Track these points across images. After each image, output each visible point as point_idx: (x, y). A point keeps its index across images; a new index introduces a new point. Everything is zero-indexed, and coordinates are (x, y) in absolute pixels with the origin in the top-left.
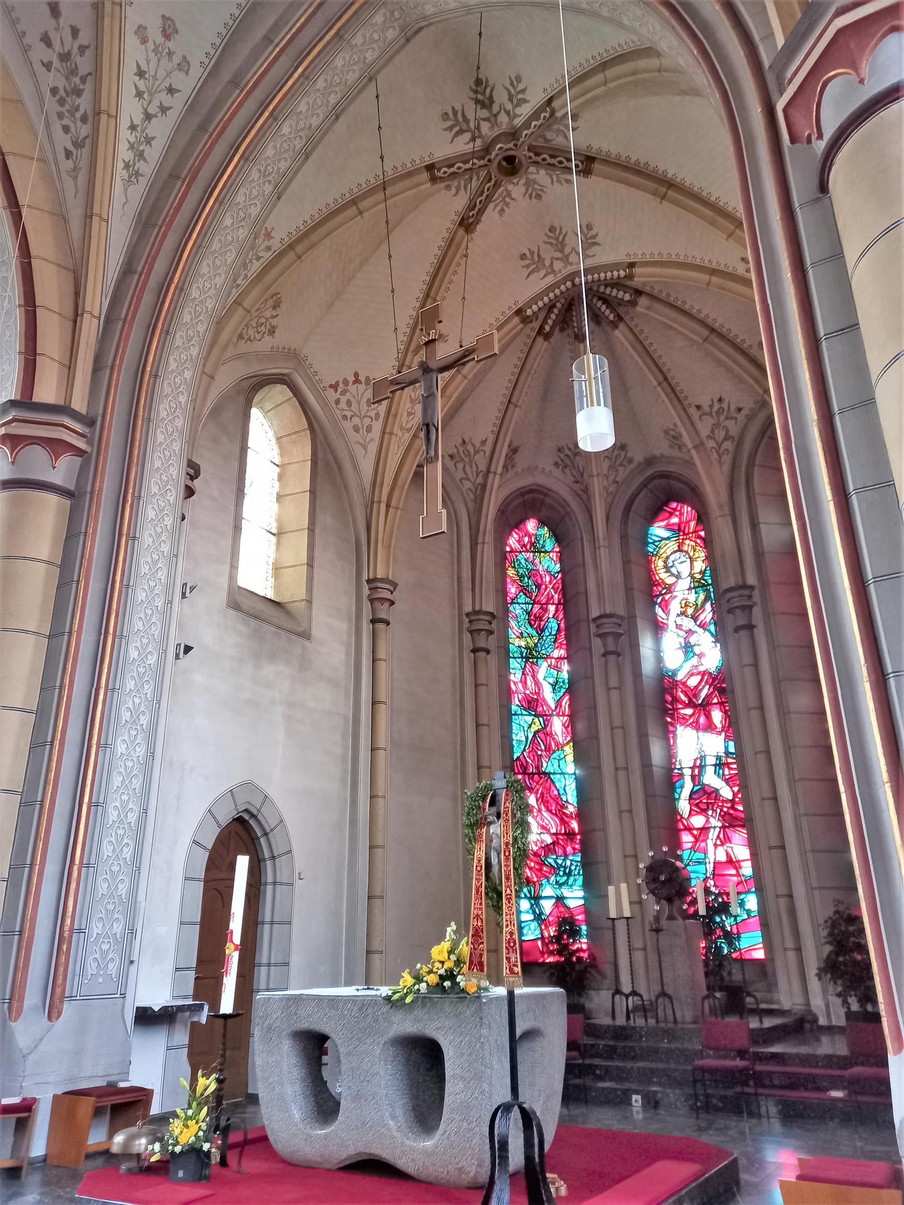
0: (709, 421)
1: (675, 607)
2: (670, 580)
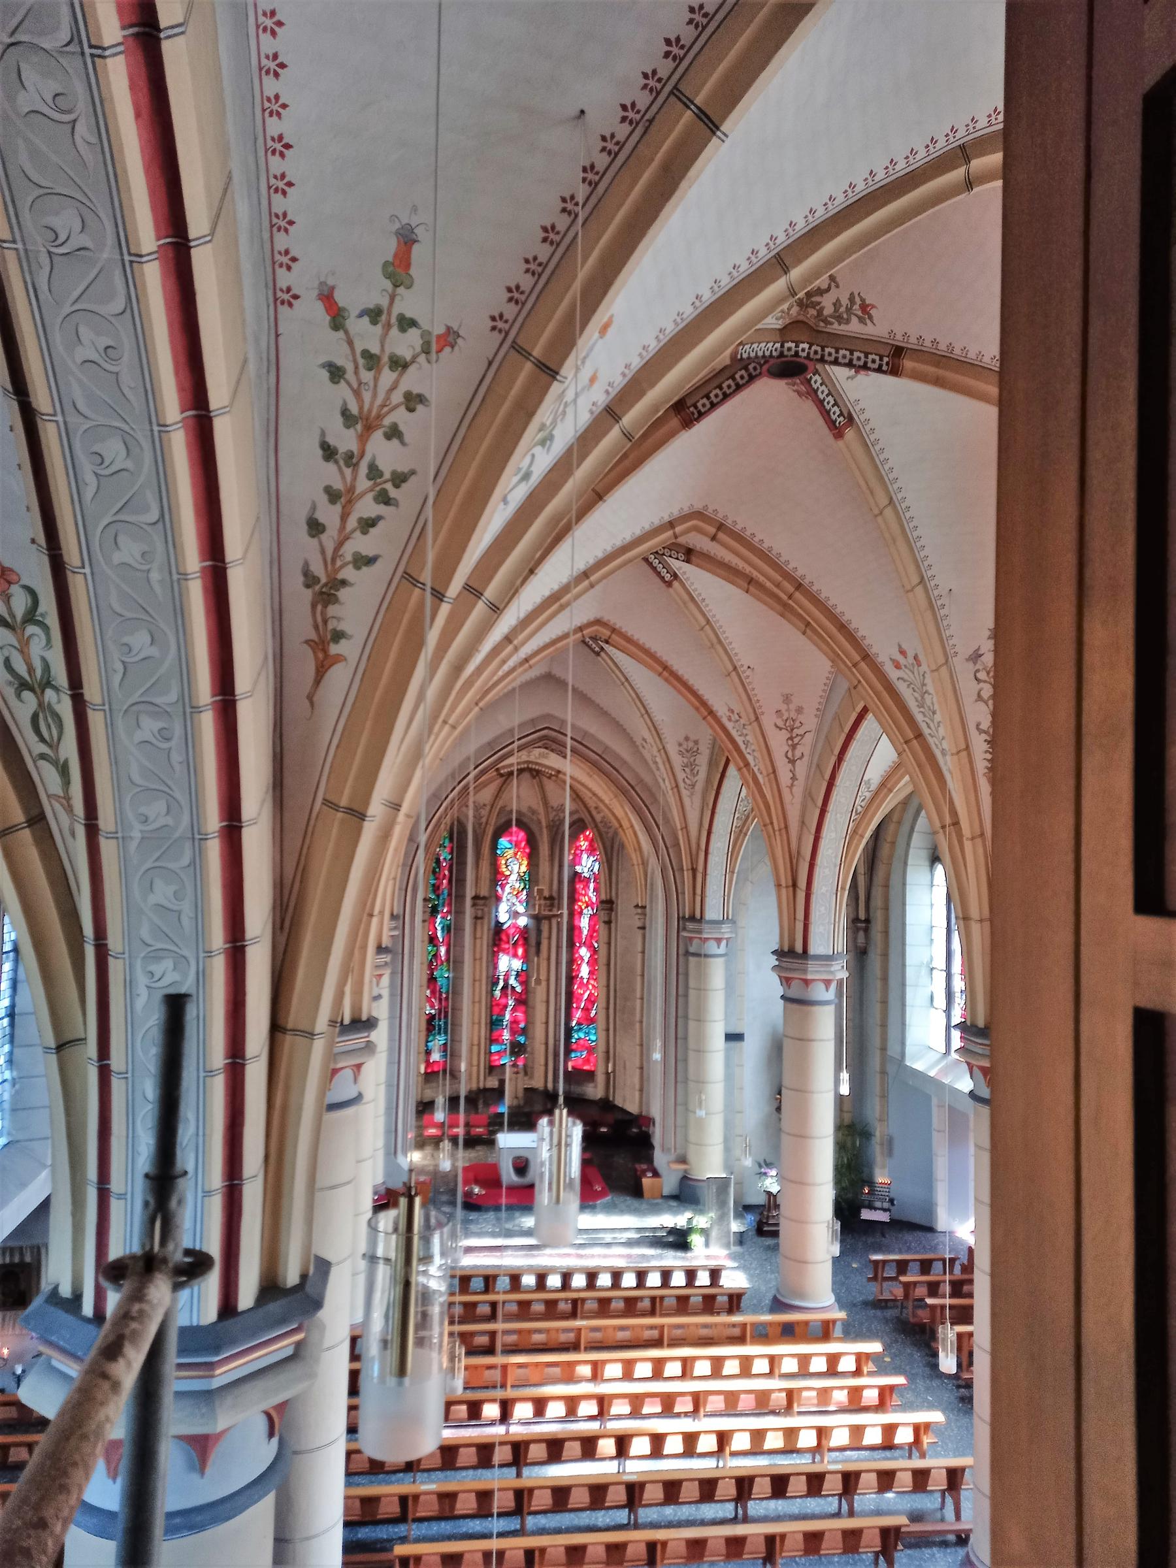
1: (508, 889)
2: (507, 873)
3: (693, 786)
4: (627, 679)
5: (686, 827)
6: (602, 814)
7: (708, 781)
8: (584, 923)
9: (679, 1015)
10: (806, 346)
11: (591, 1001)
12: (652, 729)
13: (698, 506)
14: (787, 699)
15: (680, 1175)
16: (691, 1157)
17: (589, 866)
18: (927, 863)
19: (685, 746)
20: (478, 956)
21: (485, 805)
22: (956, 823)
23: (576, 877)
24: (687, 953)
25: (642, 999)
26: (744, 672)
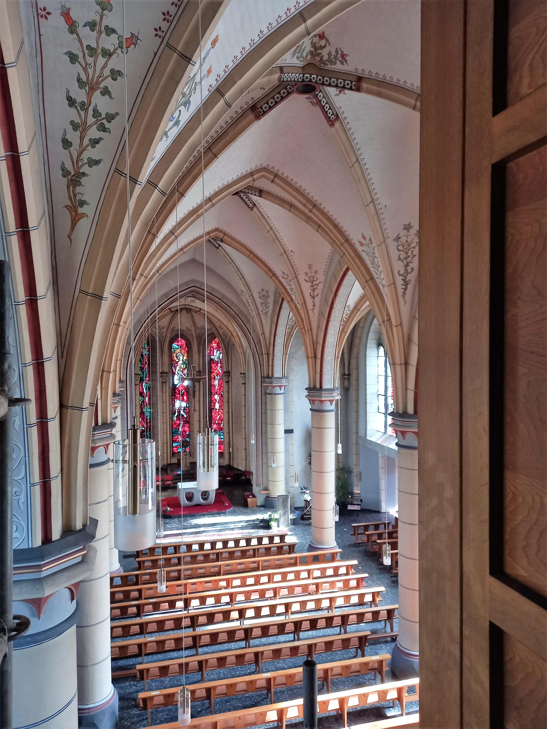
0: (199, 330)
1: (178, 368)
2: (177, 360)
3: (267, 313)
4: (232, 261)
5: (264, 333)
6: (223, 330)
7: (274, 310)
8: (216, 383)
9: (263, 422)
10: (315, 76)
11: (221, 419)
12: (246, 285)
13: (265, 165)
14: (310, 267)
15: (265, 496)
16: (270, 488)
17: (217, 356)
18: (376, 346)
19: (262, 294)
20: (164, 401)
21: (164, 327)
22: (389, 320)
23: (211, 361)
24: (266, 394)
25: (245, 417)
26: (289, 253)
